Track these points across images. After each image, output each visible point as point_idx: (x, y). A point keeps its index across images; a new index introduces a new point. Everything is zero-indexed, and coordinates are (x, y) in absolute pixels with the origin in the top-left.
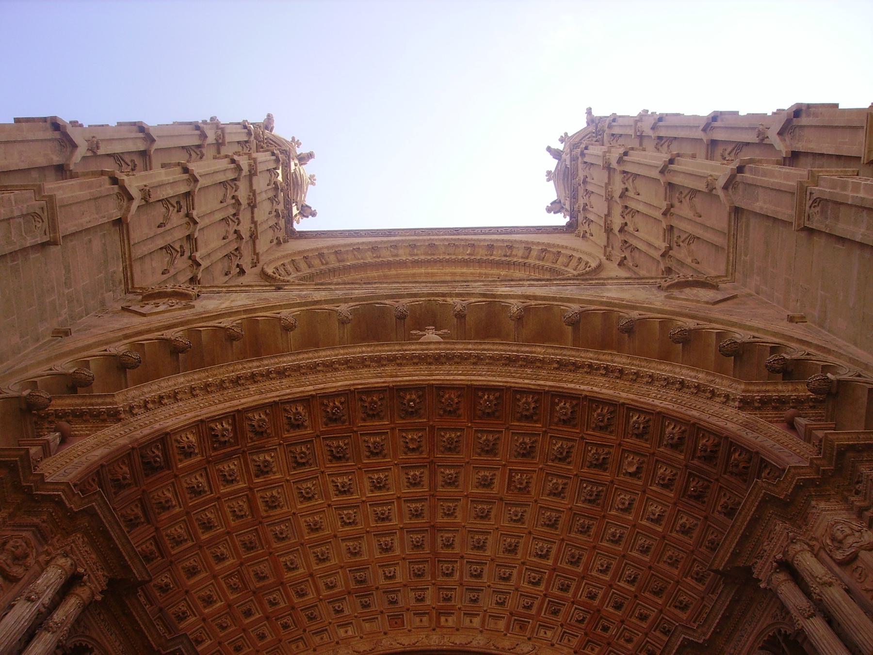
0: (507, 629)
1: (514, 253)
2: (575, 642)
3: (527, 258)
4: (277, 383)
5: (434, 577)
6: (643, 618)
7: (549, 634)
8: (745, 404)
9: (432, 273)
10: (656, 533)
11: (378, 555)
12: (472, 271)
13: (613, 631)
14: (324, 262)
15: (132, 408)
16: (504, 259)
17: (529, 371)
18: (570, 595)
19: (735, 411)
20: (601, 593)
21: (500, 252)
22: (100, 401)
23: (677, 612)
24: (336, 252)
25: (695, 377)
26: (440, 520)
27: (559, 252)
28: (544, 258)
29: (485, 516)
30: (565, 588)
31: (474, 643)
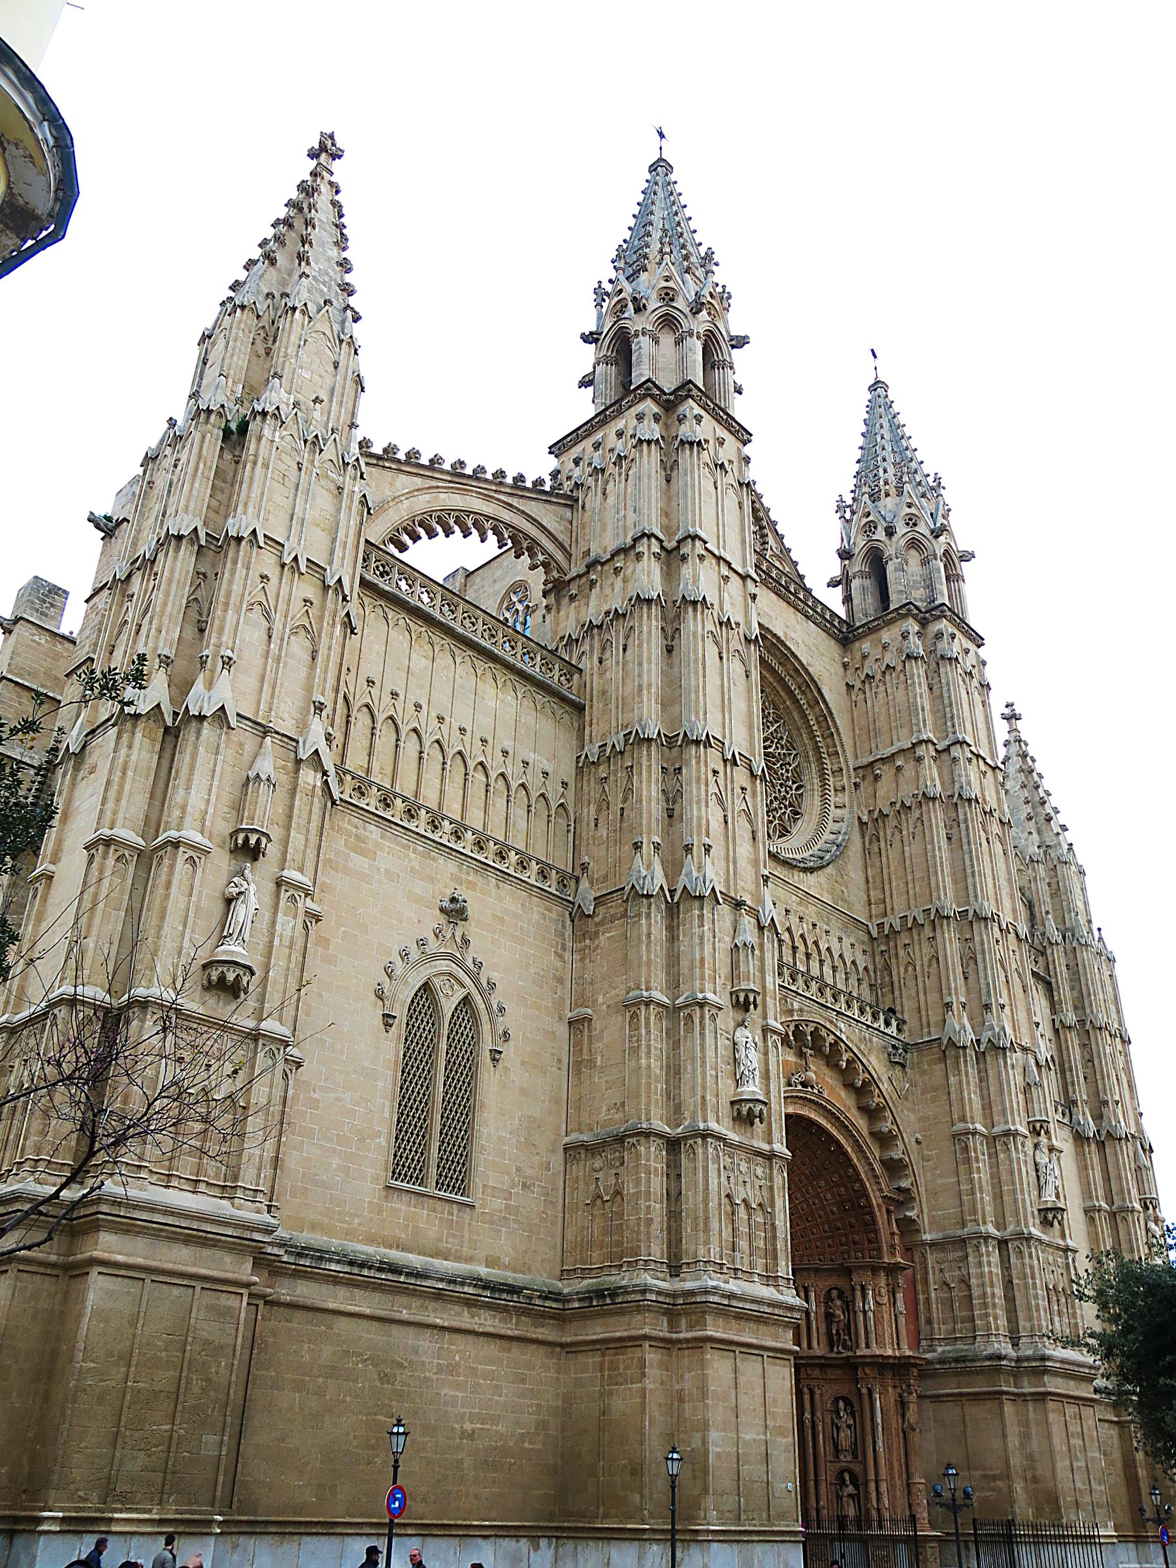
8: (884, 1197)
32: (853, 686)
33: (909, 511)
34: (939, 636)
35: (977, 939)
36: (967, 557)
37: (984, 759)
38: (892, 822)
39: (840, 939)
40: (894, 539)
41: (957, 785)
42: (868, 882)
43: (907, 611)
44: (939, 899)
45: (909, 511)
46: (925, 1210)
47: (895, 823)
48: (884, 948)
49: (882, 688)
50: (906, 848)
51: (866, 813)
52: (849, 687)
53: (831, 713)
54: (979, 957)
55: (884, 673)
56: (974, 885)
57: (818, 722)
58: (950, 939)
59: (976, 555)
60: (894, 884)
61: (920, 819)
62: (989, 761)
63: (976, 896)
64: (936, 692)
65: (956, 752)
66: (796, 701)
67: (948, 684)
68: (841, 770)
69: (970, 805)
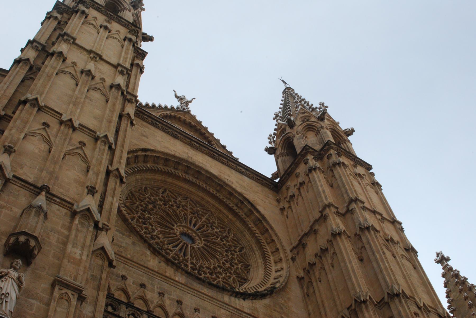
3: (248, 216)
9: (192, 192)
14: (137, 162)
16: (235, 208)
24: (145, 155)
28: (257, 224)
32: (284, 208)
33: (303, 115)
34: (329, 157)
36: (350, 132)
37: (381, 215)
38: (318, 266)
40: (295, 128)
41: (357, 224)
45: (303, 115)
47: (320, 266)
49: (300, 198)
50: (329, 276)
52: (282, 210)
53: (264, 217)
55: (299, 189)
56: (384, 279)
57: (256, 225)
59: (355, 129)
60: (326, 305)
61: (335, 253)
62: (385, 215)
64: (335, 185)
65: (353, 205)
66: (235, 214)
67: (340, 177)
68: (277, 250)
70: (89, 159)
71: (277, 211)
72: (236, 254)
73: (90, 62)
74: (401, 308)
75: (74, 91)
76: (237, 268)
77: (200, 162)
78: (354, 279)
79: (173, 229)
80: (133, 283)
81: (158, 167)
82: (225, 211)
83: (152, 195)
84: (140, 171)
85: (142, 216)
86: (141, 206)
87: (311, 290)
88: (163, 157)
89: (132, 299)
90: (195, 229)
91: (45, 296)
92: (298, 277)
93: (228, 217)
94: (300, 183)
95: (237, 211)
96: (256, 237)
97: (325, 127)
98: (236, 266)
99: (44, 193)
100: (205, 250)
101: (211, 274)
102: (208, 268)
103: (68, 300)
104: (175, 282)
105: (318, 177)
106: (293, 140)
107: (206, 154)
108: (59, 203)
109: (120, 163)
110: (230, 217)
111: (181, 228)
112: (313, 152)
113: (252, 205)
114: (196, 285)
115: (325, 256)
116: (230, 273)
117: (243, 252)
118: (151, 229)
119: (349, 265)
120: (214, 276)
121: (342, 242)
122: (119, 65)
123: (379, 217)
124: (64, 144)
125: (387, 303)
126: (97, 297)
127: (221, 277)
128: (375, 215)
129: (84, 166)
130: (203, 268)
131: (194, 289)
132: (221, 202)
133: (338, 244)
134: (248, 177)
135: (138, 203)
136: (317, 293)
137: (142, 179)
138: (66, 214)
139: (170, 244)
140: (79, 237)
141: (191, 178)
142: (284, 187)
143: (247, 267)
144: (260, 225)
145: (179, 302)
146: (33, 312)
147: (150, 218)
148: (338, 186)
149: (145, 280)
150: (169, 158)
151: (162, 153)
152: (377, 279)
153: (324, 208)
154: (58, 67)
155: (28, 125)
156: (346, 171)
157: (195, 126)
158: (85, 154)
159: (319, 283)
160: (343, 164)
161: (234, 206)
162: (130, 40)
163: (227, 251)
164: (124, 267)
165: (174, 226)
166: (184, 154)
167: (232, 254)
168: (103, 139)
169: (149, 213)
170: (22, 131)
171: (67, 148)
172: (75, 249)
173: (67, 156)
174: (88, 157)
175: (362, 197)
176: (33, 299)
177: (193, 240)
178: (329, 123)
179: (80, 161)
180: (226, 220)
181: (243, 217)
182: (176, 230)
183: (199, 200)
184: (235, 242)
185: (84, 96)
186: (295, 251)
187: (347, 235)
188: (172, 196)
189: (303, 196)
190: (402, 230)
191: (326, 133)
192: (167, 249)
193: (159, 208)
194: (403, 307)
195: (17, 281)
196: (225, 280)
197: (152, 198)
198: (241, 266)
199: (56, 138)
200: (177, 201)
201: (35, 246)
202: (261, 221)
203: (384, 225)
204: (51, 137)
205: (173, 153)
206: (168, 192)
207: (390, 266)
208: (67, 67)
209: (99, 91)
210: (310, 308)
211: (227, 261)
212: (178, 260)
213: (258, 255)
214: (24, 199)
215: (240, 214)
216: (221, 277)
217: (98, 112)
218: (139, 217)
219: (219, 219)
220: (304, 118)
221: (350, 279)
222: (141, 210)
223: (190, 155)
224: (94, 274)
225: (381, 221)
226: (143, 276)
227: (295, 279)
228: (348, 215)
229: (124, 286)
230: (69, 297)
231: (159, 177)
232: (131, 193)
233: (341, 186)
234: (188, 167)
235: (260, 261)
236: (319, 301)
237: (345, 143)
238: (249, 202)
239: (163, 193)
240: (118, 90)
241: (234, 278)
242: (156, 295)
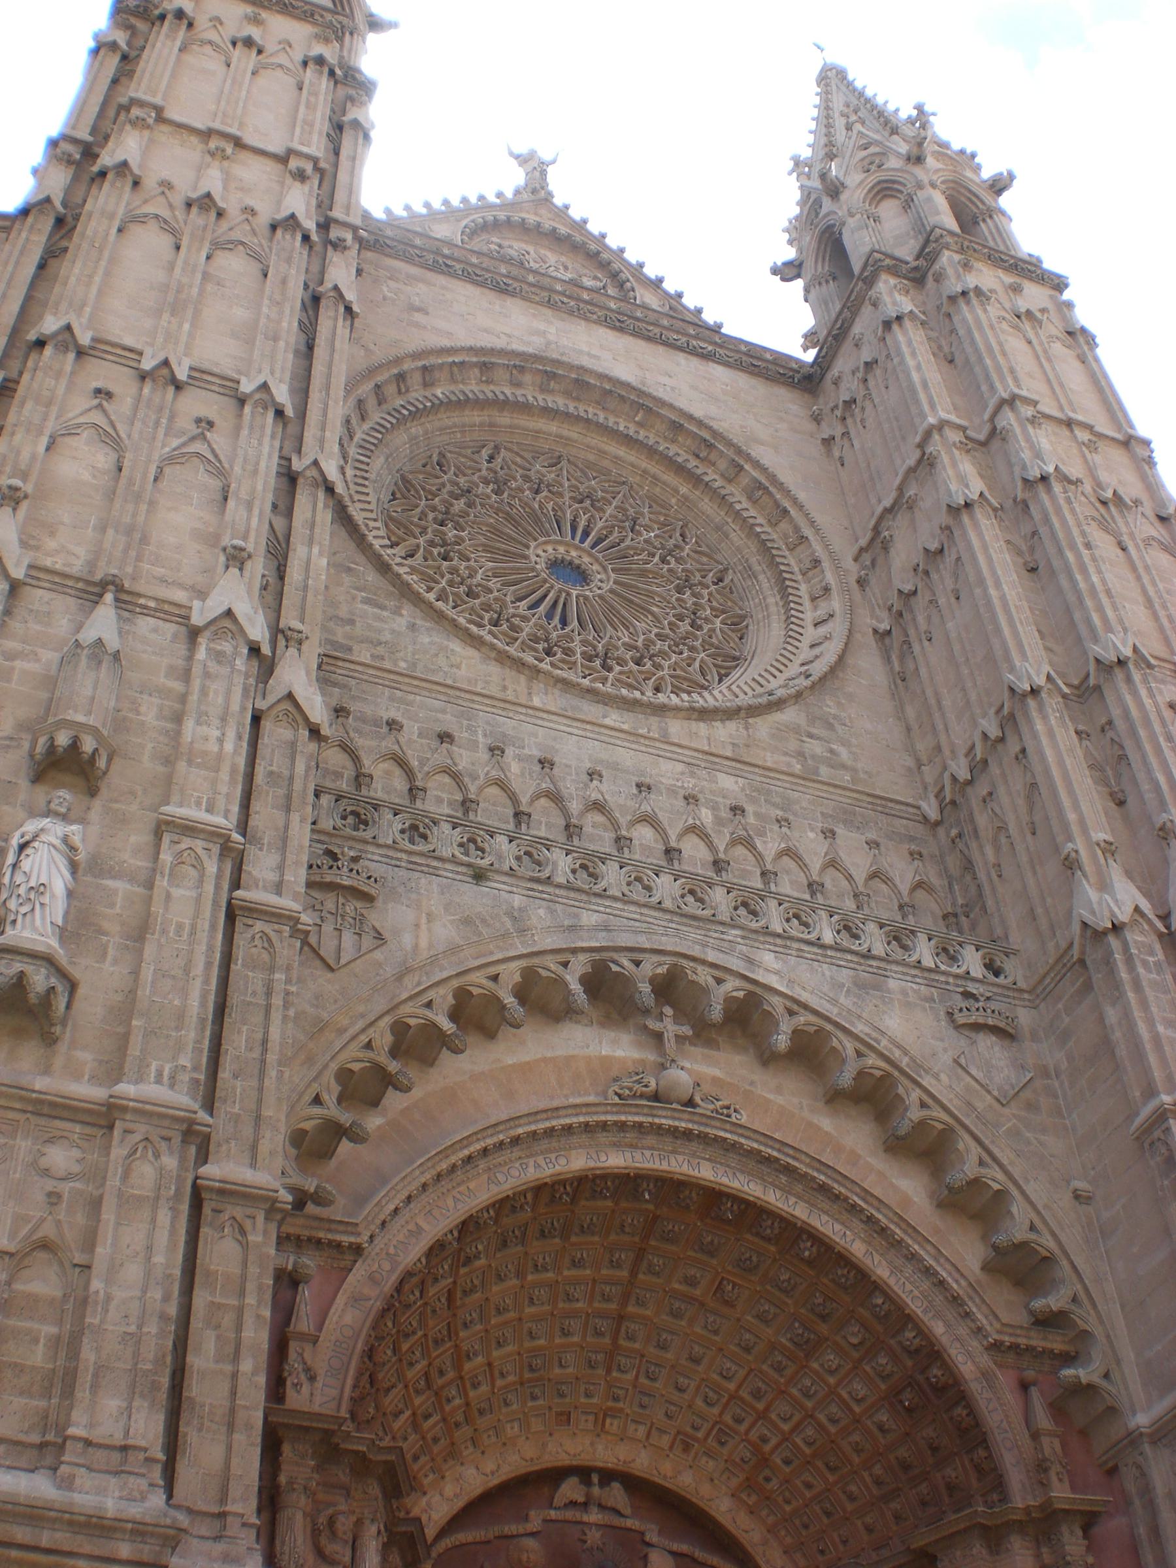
0: (671, 1448)
1: (713, 457)
2: (735, 1482)
3: (730, 481)
4: (505, 1155)
5: (609, 1371)
6: (809, 1486)
7: (711, 1463)
9: (568, 439)
10: (851, 1410)
11: (558, 1341)
12: (632, 459)
13: (774, 1484)
15: (371, 1237)
17: (784, 1179)
18: (742, 1428)
19: (980, 1348)
20: (774, 1441)
21: (689, 442)
22: (342, 1228)
23: (843, 1497)
24: (425, 369)
25: (957, 1281)
26: (631, 1309)
27: (785, 512)
29: (677, 1315)
30: (739, 1421)
31: (638, 1461)
33: (864, 153)
35: (1116, 713)
37: (1089, 428)
38: (920, 602)
39: (828, 834)
41: (1017, 470)
42: (909, 729)
43: (878, 264)
44: (1012, 669)
45: (864, 153)
46: (1128, 1354)
47: (927, 598)
48: (954, 832)
51: (884, 615)
52: (828, 442)
53: (773, 478)
54: (1128, 744)
57: (755, 502)
58: (1051, 734)
60: (947, 703)
63: (1096, 639)
64: (959, 360)
65: (1008, 418)
66: (696, 480)
68: (816, 562)
69: (1049, 490)
70: (226, 466)
71: (815, 449)
72: (705, 592)
73: (208, 166)
74: (1128, 699)
75: (171, 267)
76: (714, 630)
77: (581, 352)
78: (1006, 631)
79: (526, 557)
80: (420, 735)
81: (467, 389)
82: (669, 478)
83: (460, 472)
84: (416, 414)
85: (437, 540)
86: (434, 509)
87: (911, 666)
88: (474, 359)
89: (420, 776)
90: (586, 544)
91: (141, 863)
92: (875, 631)
93: (677, 491)
94: (866, 364)
95: (699, 472)
96: (758, 535)
97: (926, 181)
98: (706, 628)
99: (109, 597)
100: (618, 595)
101: (638, 663)
102: (629, 647)
103: (198, 865)
104: (530, 712)
105: (909, 343)
106: (840, 234)
107: (598, 322)
108: (155, 610)
109: (322, 442)
110: (684, 490)
111: (550, 548)
112: (895, 266)
113: (739, 451)
114: (591, 710)
115: (938, 571)
116: (692, 649)
117: (727, 581)
118: (467, 568)
119: (993, 592)
120: (649, 665)
121: (976, 526)
122: (290, 152)
123: (1083, 435)
124: (154, 438)
125: (1098, 688)
126: (286, 828)
127: (666, 664)
128: (1072, 431)
129: (215, 483)
130: (617, 649)
131: (583, 721)
132: (651, 452)
133: (964, 534)
134: (727, 365)
135: (423, 502)
136: (923, 671)
137: (426, 432)
138: (175, 636)
139: (520, 599)
140: (211, 694)
141: (559, 402)
142: (829, 377)
143: (738, 625)
144: (765, 498)
145: (545, 763)
146: (118, 910)
147: (459, 541)
148: (967, 361)
149: (448, 721)
150: (493, 360)
151: (471, 349)
152: (1072, 623)
153: (928, 434)
154: (121, 211)
155: (54, 410)
156: (985, 311)
157: (569, 236)
158: (213, 451)
159: (926, 643)
160: (978, 291)
161: (690, 457)
162: (320, 61)
163: (679, 590)
164: (392, 699)
165: (528, 547)
166: (535, 339)
167: (694, 595)
168: (257, 396)
169: (458, 527)
170: (40, 433)
171: (164, 446)
172: (205, 728)
173: (167, 470)
174: (222, 458)
175: (1031, 387)
176: (114, 878)
177: (582, 576)
178: (940, 166)
179: (203, 477)
180: (673, 501)
181: (716, 485)
182: (534, 558)
183: (591, 457)
184: (705, 559)
185: (199, 276)
186: (867, 558)
187: (990, 505)
188: (516, 464)
189: (876, 401)
190: (1150, 462)
191: (929, 199)
192: (514, 616)
193: (482, 505)
194: (1135, 693)
195: (63, 847)
196: (679, 672)
197: (462, 480)
198: (722, 623)
199: (132, 424)
200: (532, 474)
201: (96, 750)
202: (766, 488)
203: (1097, 459)
204: (119, 426)
205: (500, 343)
206: (503, 452)
207: (1104, 581)
208: (145, 202)
209: (241, 248)
210: (910, 712)
211: (681, 618)
212: (547, 640)
213: (766, 585)
214: (64, 622)
215: (707, 479)
216: (666, 664)
217: (240, 313)
218: (432, 543)
219: (653, 499)
220: (867, 161)
221: (998, 630)
222: (435, 519)
223: (551, 338)
224: (274, 768)
225: (1088, 447)
226: (444, 711)
227: (871, 640)
228: (996, 444)
229: (396, 747)
230: (198, 857)
231: (474, 417)
232: (403, 478)
233: (973, 359)
234: (553, 376)
235: (774, 600)
236: (929, 692)
237: (991, 217)
238: (729, 444)
239: (491, 458)
240: (294, 230)
241: (702, 661)
242: (483, 755)
